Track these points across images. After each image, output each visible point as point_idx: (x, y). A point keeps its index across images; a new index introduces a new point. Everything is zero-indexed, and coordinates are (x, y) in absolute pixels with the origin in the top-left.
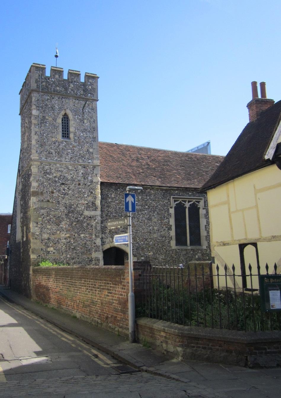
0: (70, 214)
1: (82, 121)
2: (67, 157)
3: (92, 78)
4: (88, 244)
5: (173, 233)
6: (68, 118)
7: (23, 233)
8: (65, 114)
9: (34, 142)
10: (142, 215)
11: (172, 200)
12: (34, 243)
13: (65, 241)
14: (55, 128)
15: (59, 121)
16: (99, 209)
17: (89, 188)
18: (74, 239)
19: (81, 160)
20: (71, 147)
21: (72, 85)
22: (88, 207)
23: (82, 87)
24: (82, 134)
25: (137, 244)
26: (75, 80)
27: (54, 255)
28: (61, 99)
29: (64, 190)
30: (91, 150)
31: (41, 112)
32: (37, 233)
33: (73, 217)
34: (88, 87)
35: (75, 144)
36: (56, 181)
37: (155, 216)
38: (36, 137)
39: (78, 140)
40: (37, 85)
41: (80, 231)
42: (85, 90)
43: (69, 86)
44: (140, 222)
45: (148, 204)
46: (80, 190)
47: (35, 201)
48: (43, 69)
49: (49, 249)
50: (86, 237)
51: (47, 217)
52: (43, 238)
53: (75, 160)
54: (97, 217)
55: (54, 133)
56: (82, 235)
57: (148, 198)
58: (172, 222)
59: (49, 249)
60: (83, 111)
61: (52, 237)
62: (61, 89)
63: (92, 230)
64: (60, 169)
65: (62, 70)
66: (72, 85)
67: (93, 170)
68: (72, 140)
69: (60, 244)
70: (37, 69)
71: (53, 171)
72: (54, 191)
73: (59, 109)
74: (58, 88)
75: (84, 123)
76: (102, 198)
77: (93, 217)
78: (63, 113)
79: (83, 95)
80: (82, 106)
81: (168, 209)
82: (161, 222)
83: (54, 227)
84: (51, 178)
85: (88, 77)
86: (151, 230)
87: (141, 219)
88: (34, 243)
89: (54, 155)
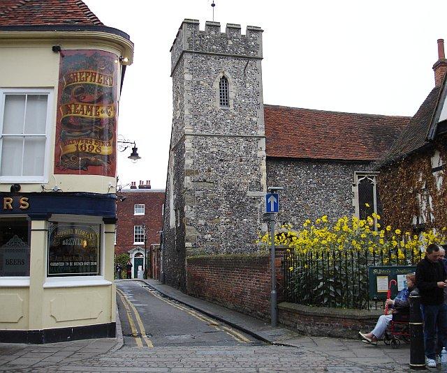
1: (243, 84)
6: (226, 81)
7: (177, 218)
8: (224, 77)
9: (187, 112)
11: (356, 177)
12: (190, 230)
15: (216, 86)
16: (265, 189)
21: (230, 42)
22: (251, 188)
24: (243, 101)
26: (235, 35)
30: (255, 119)
33: (234, 199)
38: (190, 106)
40: (190, 45)
42: (247, 48)
47: (188, 181)
48: (196, 24)
49: (206, 237)
59: (206, 237)
65: (217, 24)
66: (230, 42)
68: (232, 107)
70: (190, 24)
74: (214, 47)
76: (268, 177)
78: (221, 75)
80: (244, 67)
88: (190, 230)
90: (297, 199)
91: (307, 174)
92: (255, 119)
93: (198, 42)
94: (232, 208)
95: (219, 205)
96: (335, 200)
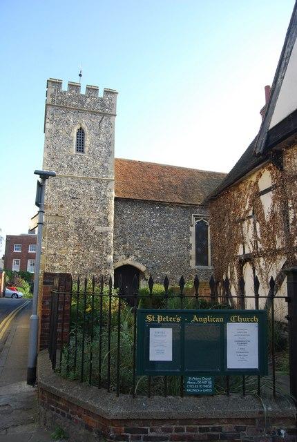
1: (98, 135)
3: (110, 93)
5: (193, 252)
8: (81, 128)
11: (193, 218)
21: (89, 100)
22: (100, 222)
30: (106, 165)
36: (66, 195)
49: (55, 265)
58: (192, 240)
66: (89, 100)
68: (87, 154)
76: (116, 214)
78: (78, 127)
81: (189, 228)
85: (107, 92)
91: (151, 214)
93: (60, 98)
96: (175, 238)
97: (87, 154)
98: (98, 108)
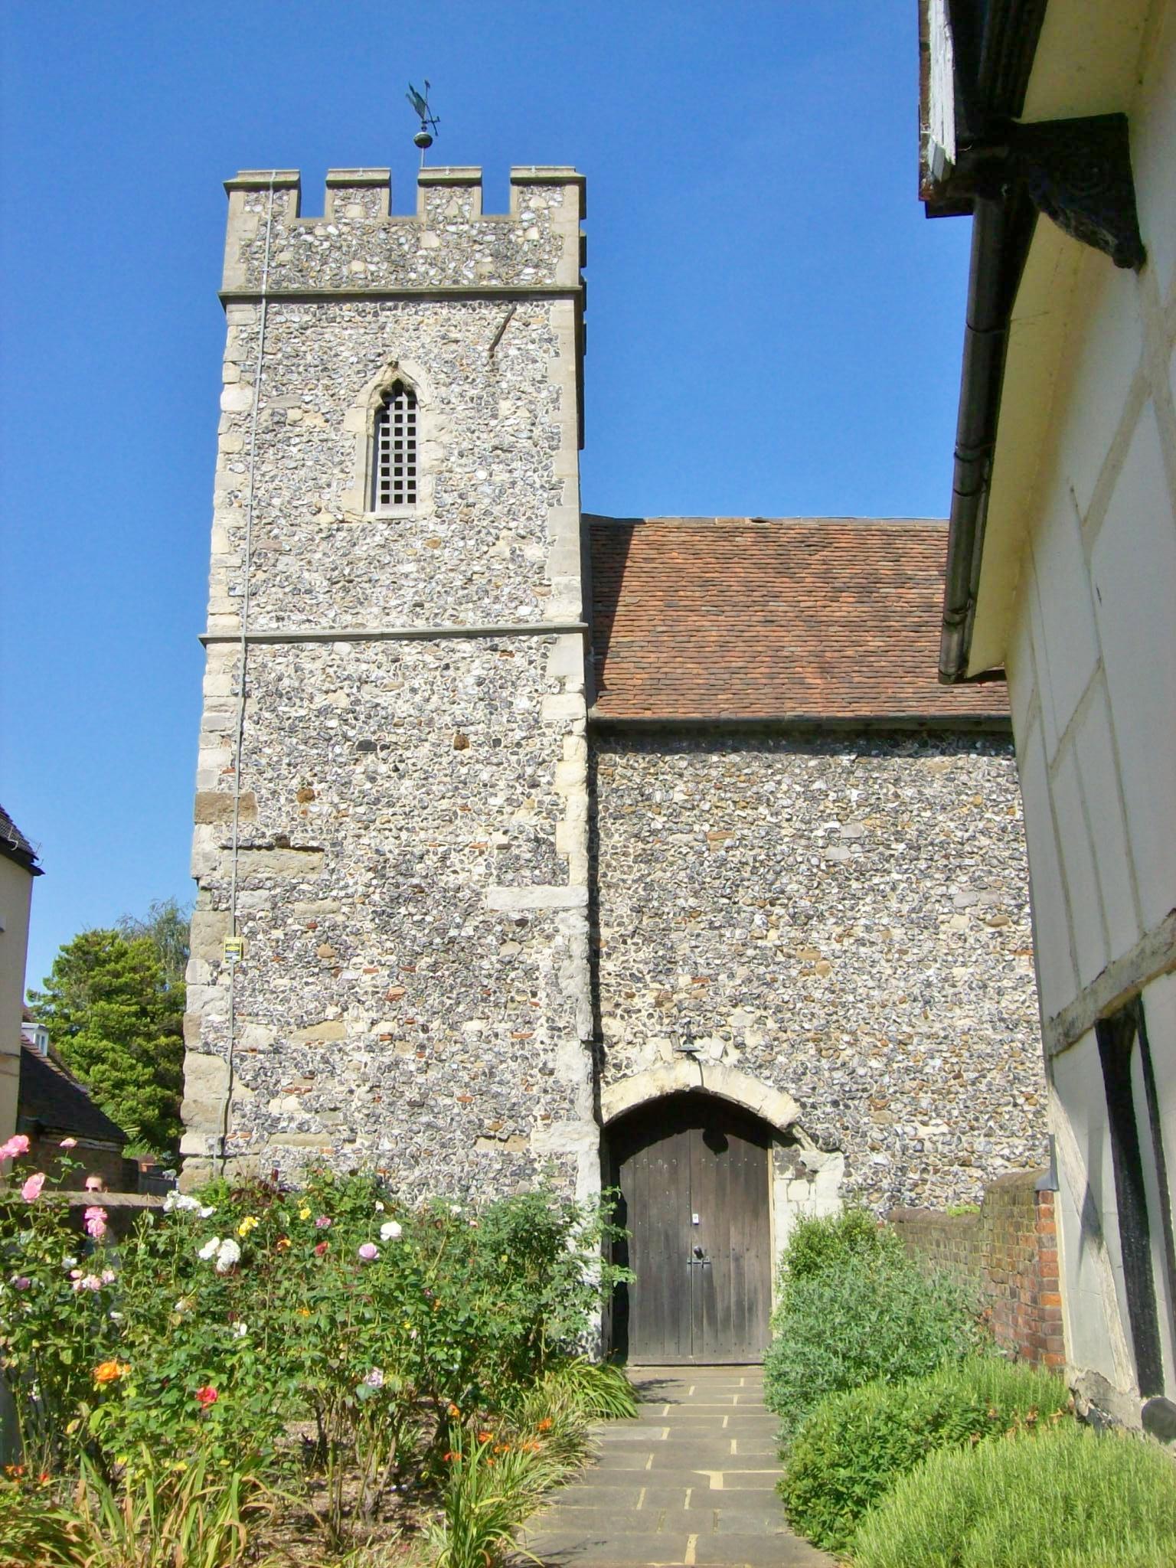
0: (403, 910)
1: (485, 406)
2: (393, 603)
4: (508, 1076)
8: (399, 387)
10: (868, 899)
13: (366, 1057)
14: (336, 460)
15: (359, 421)
16: (578, 872)
17: (514, 758)
18: (422, 1047)
19: (473, 610)
20: (419, 545)
21: (430, 240)
22: (508, 868)
23: (490, 238)
24: (482, 474)
25: (837, 1075)
26: (452, 211)
27: (302, 1136)
28: (376, 314)
29: (373, 780)
30: (533, 552)
31: (262, 395)
32: (216, 1018)
34: (520, 233)
35: (443, 531)
37: (961, 900)
39: (462, 510)
41: (458, 1003)
43: (418, 248)
44: (860, 942)
45: (911, 833)
46: (464, 770)
49: (275, 1107)
50: (496, 1035)
51: (273, 932)
52: (243, 1043)
53: (436, 615)
54: (562, 920)
55: (329, 486)
56: (472, 1026)
57: (908, 792)
59: (275, 1107)
60: (492, 356)
61: (295, 1042)
62: (373, 268)
63: (534, 994)
64: (351, 669)
66: (430, 240)
67: (545, 656)
69: (337, 1078)
71: (312, 680)
72: (317, 787)
73: (360, 367)
75: (494, 416)
77: (538, 921)
79: (491, 277)
80: (490, 333)
82: (1001, 934)
83: (307, 984)
84: (301, 719)
86: (929, 985)
87: (863, 921)
89: (321, 597)
90: (758, 919)
91: (813, 798)
92: (533, 552)
93: (285, 256)
94: (411, 968)
95: (344, 953)
96: (961, 923)
97: (424, 507)
98: (477, 270)
